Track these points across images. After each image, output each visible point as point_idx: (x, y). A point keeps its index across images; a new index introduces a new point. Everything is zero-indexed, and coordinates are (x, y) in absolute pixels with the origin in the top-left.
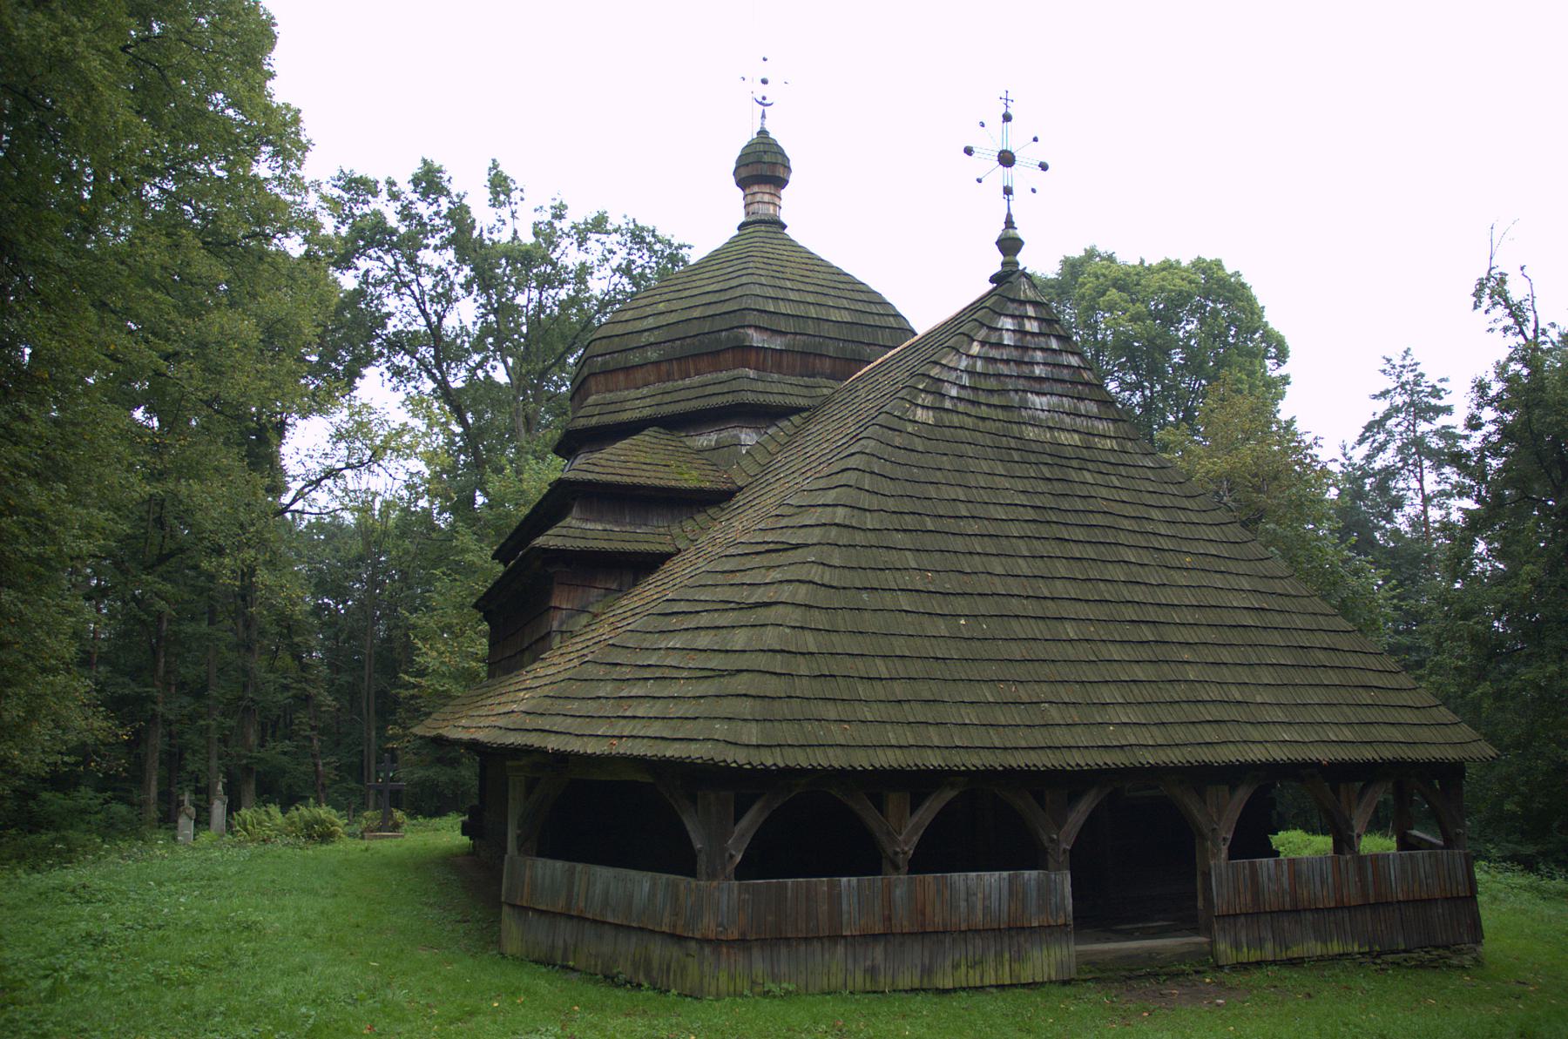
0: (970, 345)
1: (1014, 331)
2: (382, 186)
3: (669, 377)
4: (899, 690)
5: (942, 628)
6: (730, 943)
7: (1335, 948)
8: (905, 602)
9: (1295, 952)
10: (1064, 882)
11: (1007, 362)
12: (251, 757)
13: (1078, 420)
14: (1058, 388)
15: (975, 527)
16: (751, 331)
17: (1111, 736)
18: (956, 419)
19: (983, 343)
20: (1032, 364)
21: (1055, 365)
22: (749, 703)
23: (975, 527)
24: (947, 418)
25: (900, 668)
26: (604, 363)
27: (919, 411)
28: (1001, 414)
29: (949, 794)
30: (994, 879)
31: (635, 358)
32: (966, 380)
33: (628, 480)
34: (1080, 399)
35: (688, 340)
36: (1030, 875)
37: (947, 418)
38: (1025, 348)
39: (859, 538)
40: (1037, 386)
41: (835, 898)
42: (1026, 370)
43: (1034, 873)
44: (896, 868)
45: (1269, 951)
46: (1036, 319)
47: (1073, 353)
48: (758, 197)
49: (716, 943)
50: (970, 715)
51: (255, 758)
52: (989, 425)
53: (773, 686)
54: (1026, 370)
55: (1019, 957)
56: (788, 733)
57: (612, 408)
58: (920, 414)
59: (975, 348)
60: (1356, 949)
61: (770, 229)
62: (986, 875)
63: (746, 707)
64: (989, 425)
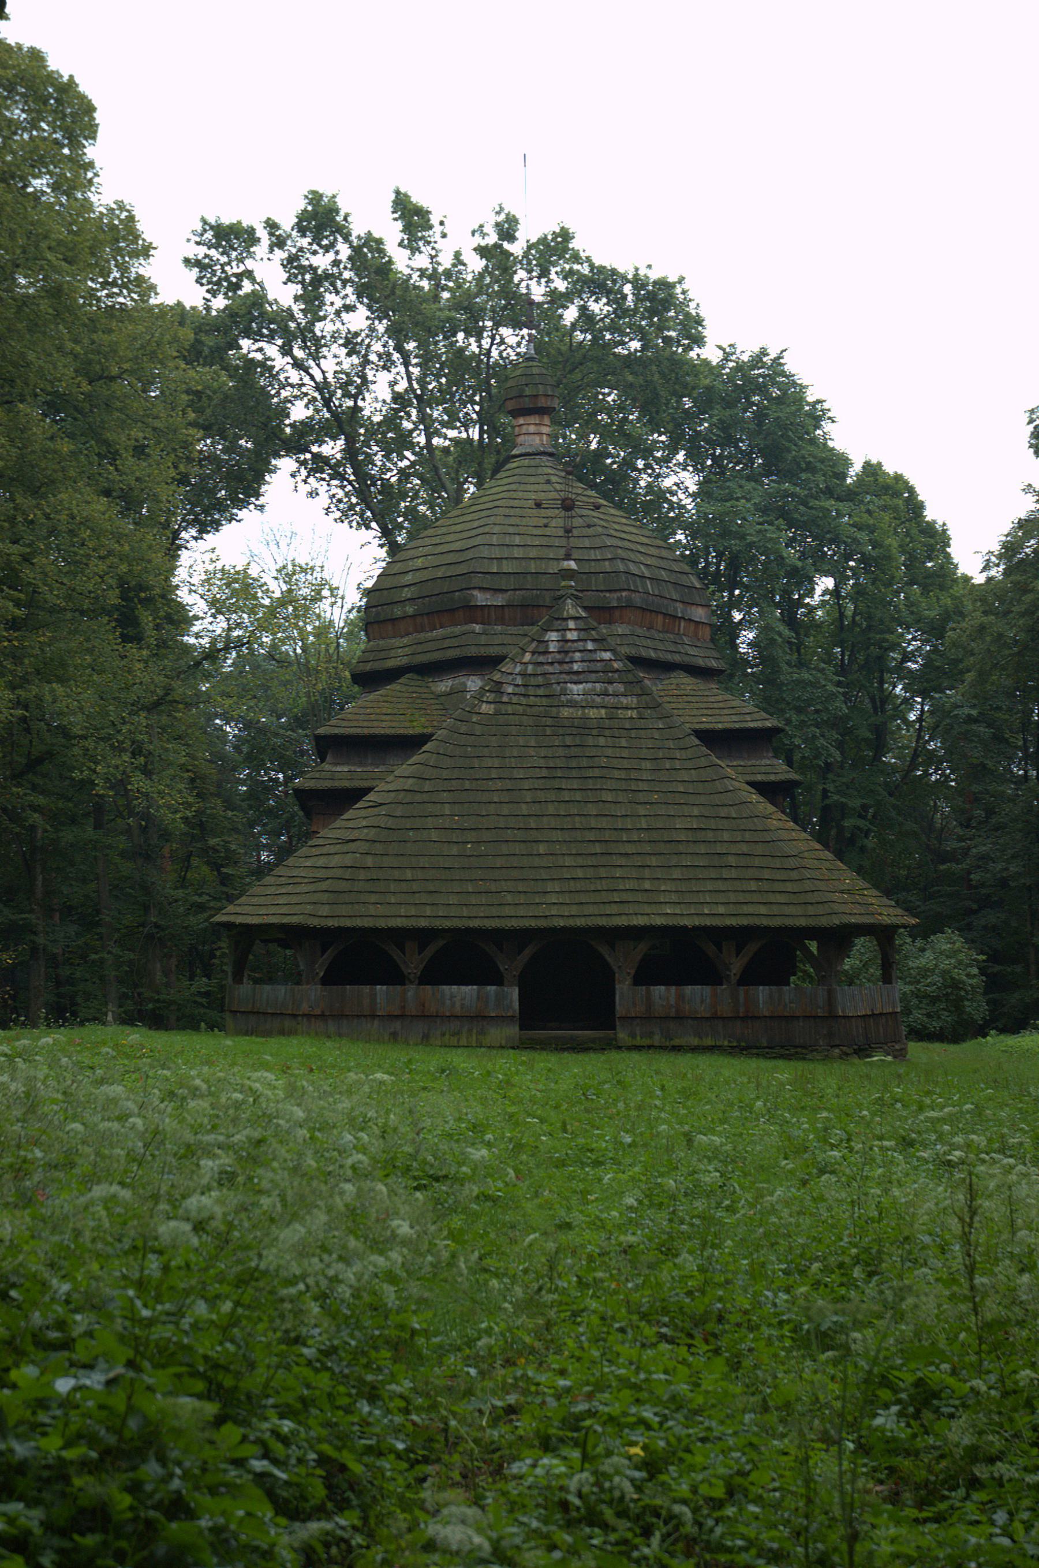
0: (523, 655)
2: (262, 233)
3: (421, 629)
4: (415, 887)
5: (455, 850)
6: (316, 1016)
7: (709, 1042)
8: (434, 835)
9: (676, 1042)
10: (515, 993)
11: (552, 663)
12: (158, 1001)
13: (607, 699)
14: (593, 677)
15: (499, 785)
16: (475, 593)
17: (540, 911)
18: (510, 709)
19: (533, 653)
20: (572, 662)
22: (327, 895)
23: (499, 785)
24: (503, 708)
25: (420, 875)
26: (378, 614)
27: (484, 706)
28: (545, 701)
29: (441, 943)
30: (469, 991)
31: (398, 612)
32: (519, 681)
33: (366, 731)
34: (610, 683)
35: (434, 598)
36: (492, 989)
37: (503, 708)
38: (567, 652)
39: (418, 798)
40: (575, 678)
41: (373, 996)
42: (566, 667)
43: (494, 988)
44: (412, 982)
45: (657, 1040)
48: (524, 429)
49: (308, 1016)
50: (453, 900)
51: (164, 1001)
52: (535, 710)
53: (343, 886)
54: (566, 667)
55: (482, 1032)
56: (344, 910)
57: (383, 655)
58: (485, 708)
59: (527, 657)
60: (726, 1043)
61: (533, 463)
62: (463, 988)
63: (325, 897)
64: (535, 710)
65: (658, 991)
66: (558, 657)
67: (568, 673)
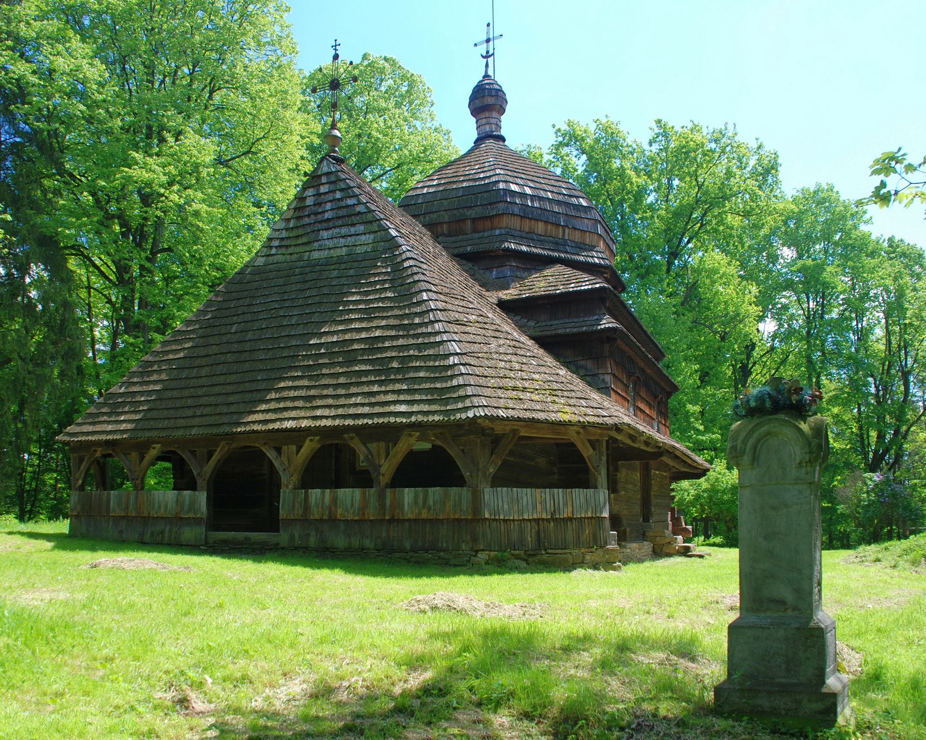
1: (314, 195)
10: (202, 497)
11: (309, 216)
20: (324, 212)
21: (339, 208)
34: (353, 225)
36: (187, 493)
40: (324, 225)
42: (320, 217)
46: (327, 183)
47: (350, 197)
54: (320, 217)
65: (315, 494)
66: (313, 208)
67: (320, 222)
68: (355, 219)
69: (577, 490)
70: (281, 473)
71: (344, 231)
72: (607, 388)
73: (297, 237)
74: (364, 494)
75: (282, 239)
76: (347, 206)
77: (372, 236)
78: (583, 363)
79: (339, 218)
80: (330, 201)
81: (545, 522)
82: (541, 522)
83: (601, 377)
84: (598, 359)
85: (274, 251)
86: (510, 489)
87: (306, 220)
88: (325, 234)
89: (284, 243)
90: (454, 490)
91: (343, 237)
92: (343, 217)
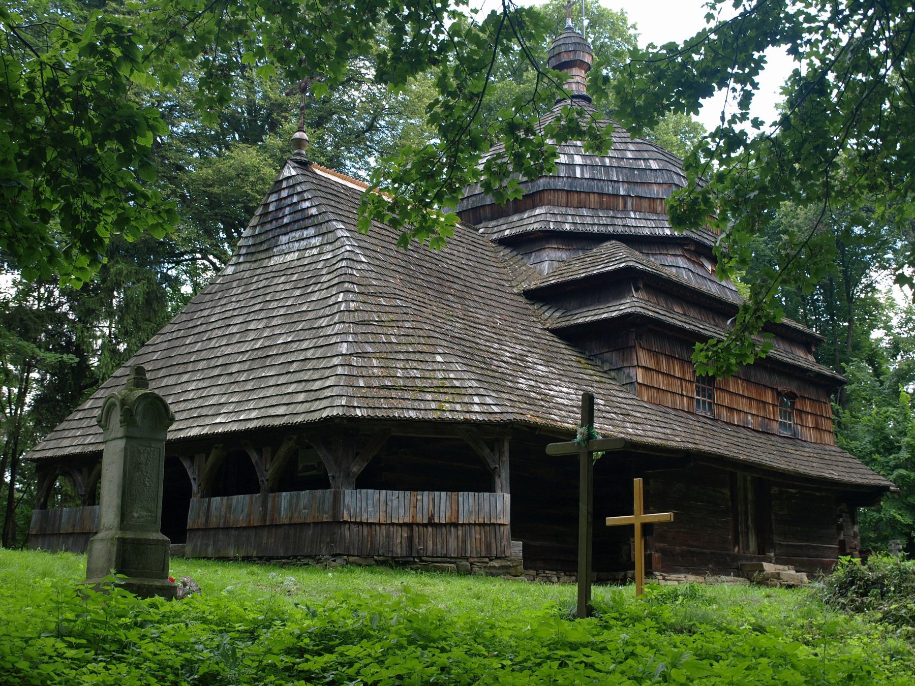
20: (283, 217)
34: (306, 228)
40: (283, 230)
65: (216, 500)
67: (280, 227)
68: (308, 222)
69: (466, 493)
70: (192, 481)
71: (297, 235)
72: (631, 383)
73: (261, 243)
74: (251, 499)
75: (249, 246)
76: (303, 210)
77: (320, 238)
78: (607, 355)
79: (295, 222)
80: (289, 205)
81: (421, 528)
82: (416, 528)
83: (626, 371)
84: (625, 350)
85: (241, 260)
86: (377, 491)
87: (268, 227)
88: (284, 239)
89: (249, 251)
90: (319, 492)
91: (297, 241)
92: (298, 221)
